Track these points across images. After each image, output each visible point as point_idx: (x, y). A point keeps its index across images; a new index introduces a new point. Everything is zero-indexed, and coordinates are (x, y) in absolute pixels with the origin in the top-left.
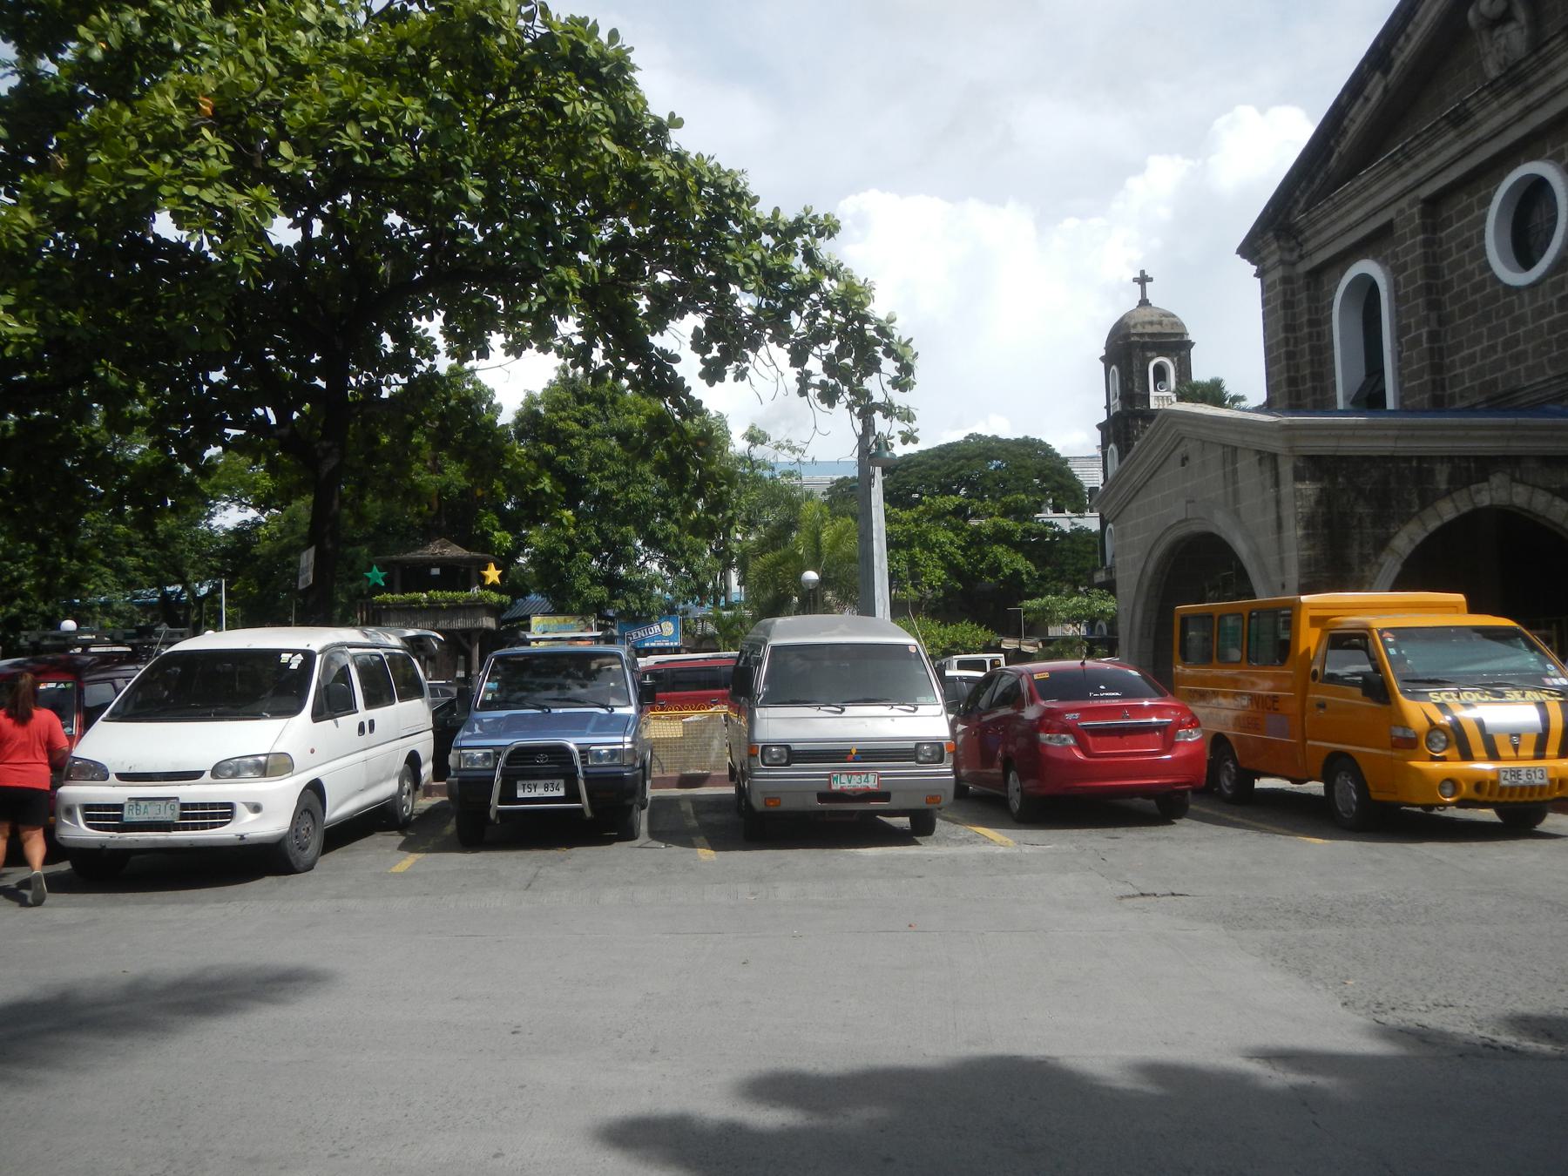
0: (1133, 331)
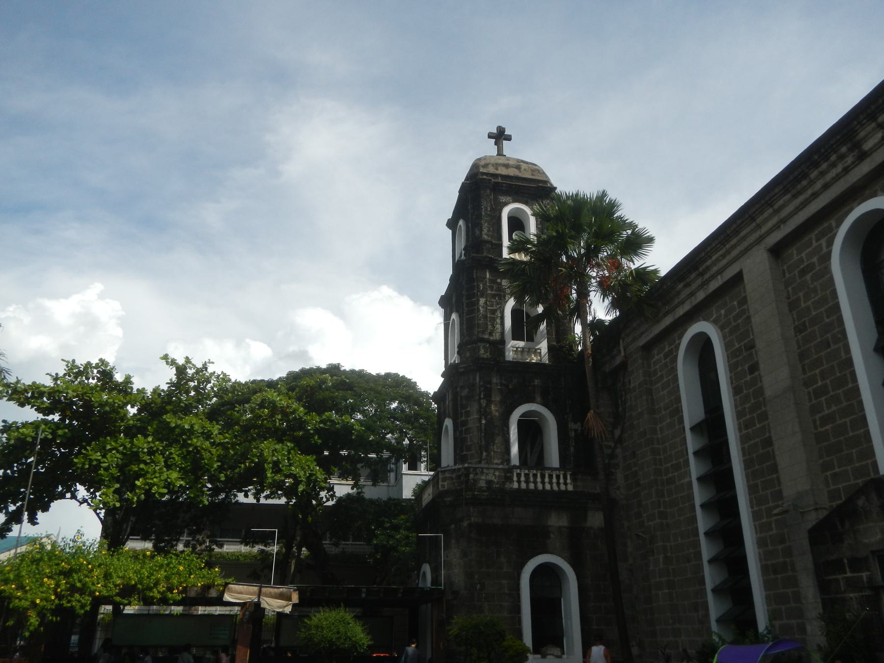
0: (482, 170)
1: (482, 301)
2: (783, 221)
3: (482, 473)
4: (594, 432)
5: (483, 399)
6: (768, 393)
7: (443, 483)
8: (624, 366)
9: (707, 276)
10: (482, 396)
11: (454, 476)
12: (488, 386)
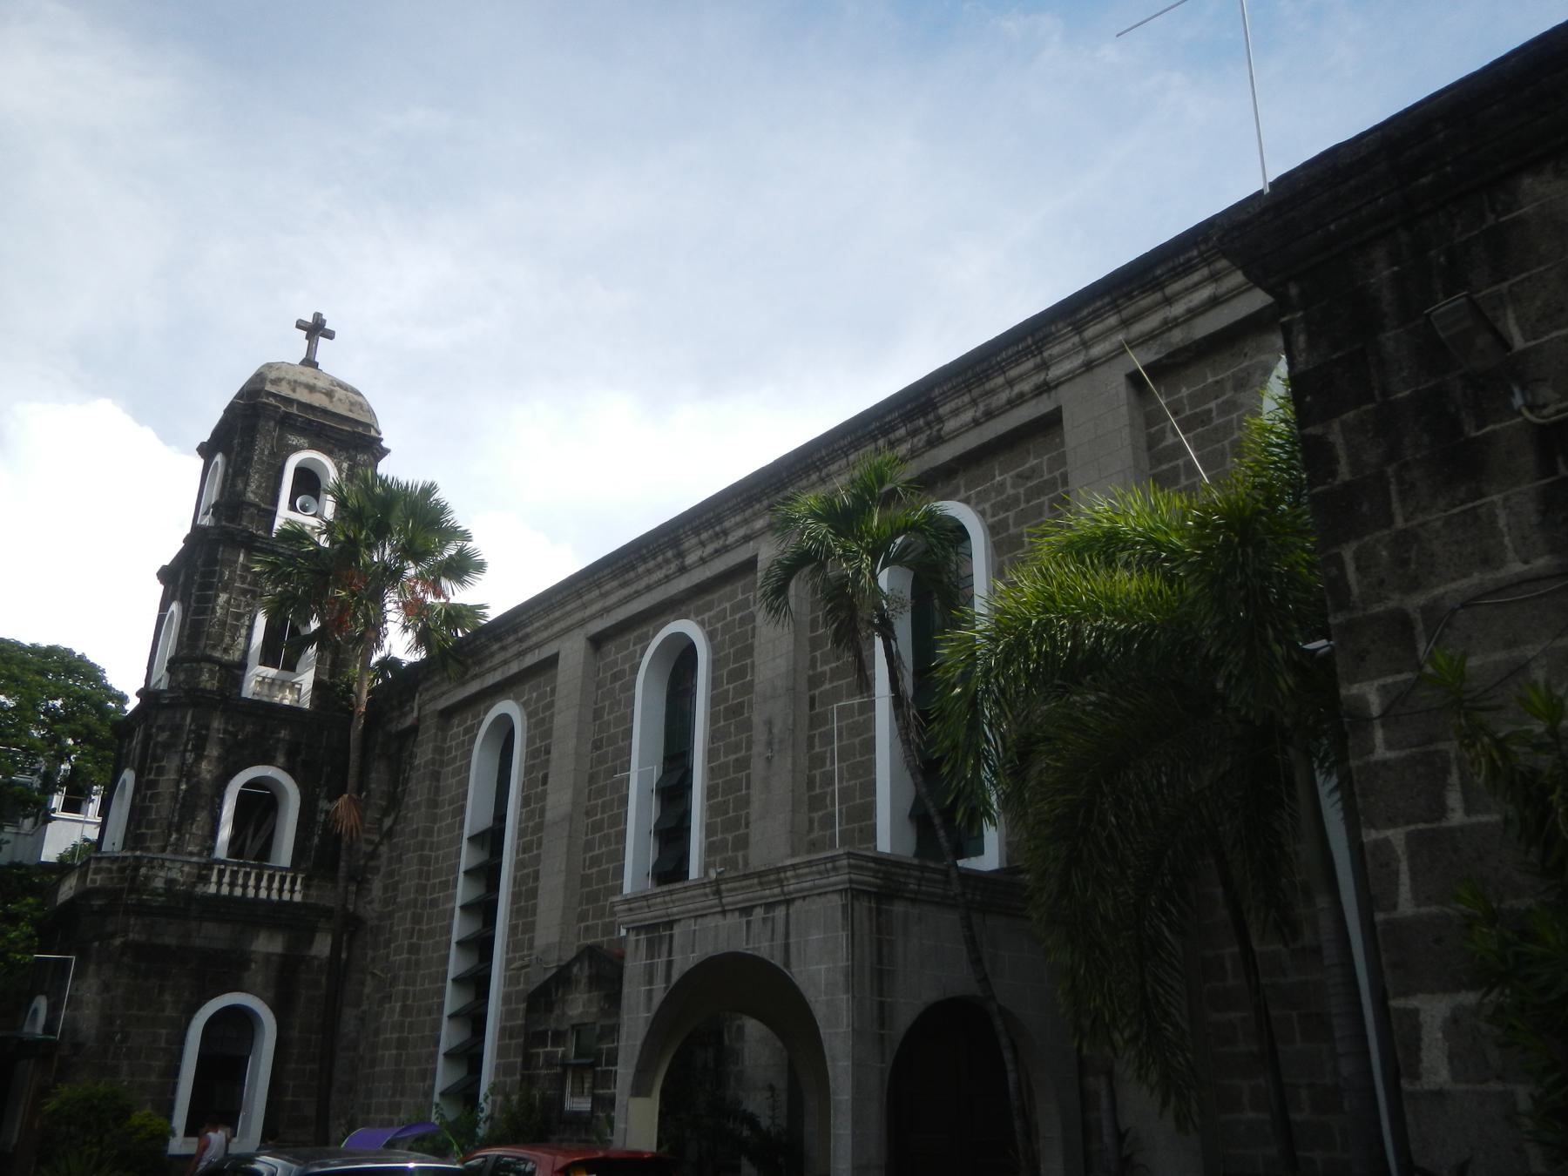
0: (269, 387)
1: (223, 597)
2: (606, 610)
3: (162, 866)
4: (342, 827)
5: (191, 751)
6: (549, 815)
7: (95, 877)
8: (414, 730)
9: (525, 645)
10: (190, 747)
11: (115, 867)
12: (204, 732)
